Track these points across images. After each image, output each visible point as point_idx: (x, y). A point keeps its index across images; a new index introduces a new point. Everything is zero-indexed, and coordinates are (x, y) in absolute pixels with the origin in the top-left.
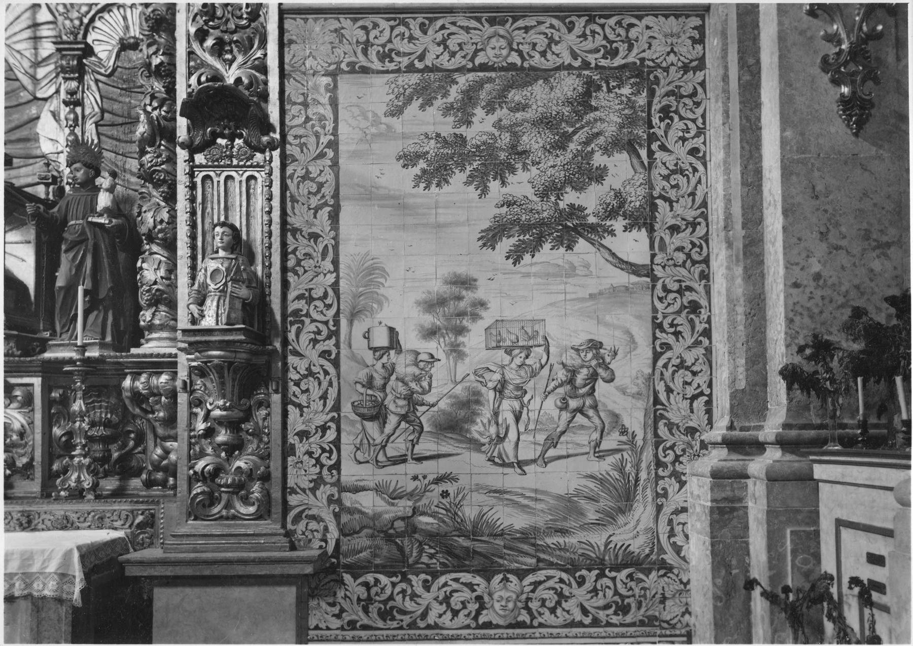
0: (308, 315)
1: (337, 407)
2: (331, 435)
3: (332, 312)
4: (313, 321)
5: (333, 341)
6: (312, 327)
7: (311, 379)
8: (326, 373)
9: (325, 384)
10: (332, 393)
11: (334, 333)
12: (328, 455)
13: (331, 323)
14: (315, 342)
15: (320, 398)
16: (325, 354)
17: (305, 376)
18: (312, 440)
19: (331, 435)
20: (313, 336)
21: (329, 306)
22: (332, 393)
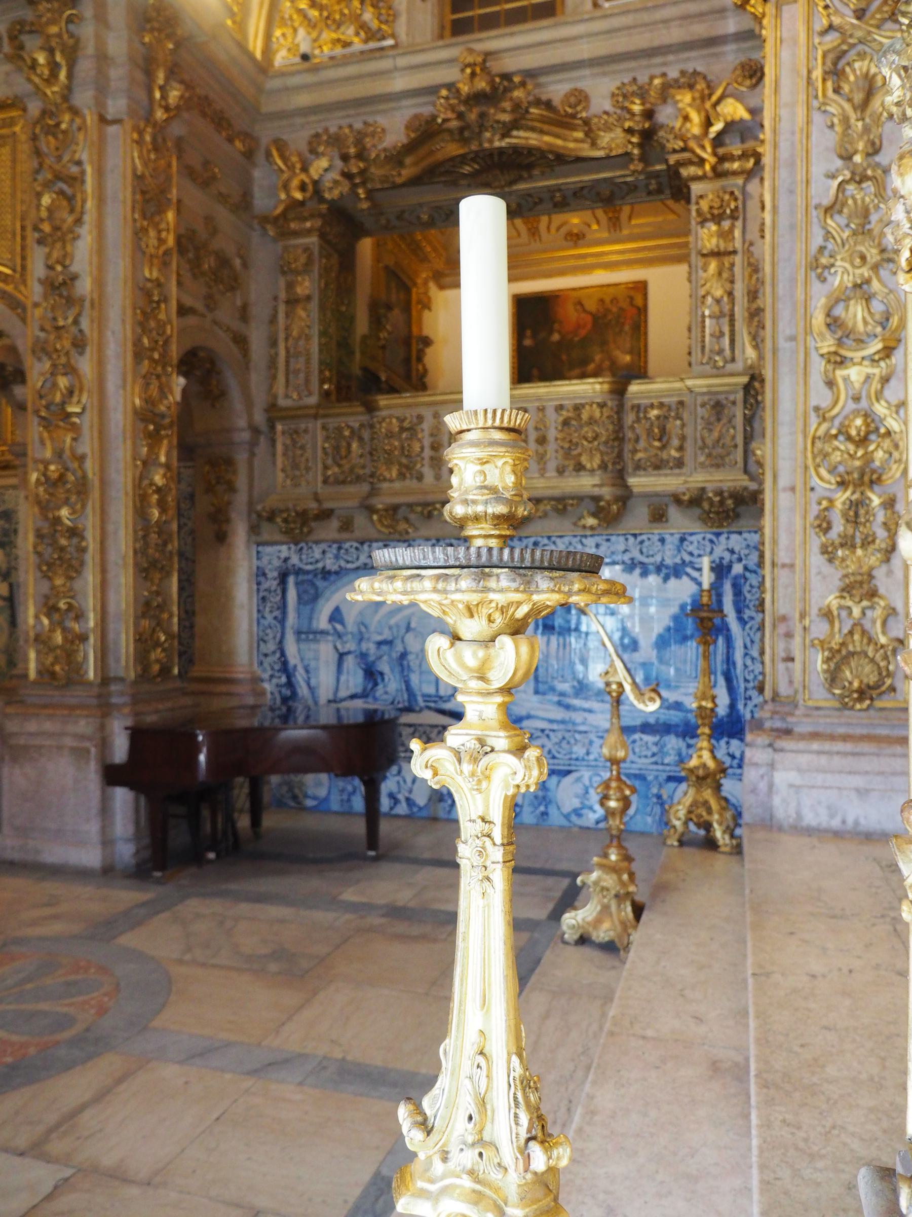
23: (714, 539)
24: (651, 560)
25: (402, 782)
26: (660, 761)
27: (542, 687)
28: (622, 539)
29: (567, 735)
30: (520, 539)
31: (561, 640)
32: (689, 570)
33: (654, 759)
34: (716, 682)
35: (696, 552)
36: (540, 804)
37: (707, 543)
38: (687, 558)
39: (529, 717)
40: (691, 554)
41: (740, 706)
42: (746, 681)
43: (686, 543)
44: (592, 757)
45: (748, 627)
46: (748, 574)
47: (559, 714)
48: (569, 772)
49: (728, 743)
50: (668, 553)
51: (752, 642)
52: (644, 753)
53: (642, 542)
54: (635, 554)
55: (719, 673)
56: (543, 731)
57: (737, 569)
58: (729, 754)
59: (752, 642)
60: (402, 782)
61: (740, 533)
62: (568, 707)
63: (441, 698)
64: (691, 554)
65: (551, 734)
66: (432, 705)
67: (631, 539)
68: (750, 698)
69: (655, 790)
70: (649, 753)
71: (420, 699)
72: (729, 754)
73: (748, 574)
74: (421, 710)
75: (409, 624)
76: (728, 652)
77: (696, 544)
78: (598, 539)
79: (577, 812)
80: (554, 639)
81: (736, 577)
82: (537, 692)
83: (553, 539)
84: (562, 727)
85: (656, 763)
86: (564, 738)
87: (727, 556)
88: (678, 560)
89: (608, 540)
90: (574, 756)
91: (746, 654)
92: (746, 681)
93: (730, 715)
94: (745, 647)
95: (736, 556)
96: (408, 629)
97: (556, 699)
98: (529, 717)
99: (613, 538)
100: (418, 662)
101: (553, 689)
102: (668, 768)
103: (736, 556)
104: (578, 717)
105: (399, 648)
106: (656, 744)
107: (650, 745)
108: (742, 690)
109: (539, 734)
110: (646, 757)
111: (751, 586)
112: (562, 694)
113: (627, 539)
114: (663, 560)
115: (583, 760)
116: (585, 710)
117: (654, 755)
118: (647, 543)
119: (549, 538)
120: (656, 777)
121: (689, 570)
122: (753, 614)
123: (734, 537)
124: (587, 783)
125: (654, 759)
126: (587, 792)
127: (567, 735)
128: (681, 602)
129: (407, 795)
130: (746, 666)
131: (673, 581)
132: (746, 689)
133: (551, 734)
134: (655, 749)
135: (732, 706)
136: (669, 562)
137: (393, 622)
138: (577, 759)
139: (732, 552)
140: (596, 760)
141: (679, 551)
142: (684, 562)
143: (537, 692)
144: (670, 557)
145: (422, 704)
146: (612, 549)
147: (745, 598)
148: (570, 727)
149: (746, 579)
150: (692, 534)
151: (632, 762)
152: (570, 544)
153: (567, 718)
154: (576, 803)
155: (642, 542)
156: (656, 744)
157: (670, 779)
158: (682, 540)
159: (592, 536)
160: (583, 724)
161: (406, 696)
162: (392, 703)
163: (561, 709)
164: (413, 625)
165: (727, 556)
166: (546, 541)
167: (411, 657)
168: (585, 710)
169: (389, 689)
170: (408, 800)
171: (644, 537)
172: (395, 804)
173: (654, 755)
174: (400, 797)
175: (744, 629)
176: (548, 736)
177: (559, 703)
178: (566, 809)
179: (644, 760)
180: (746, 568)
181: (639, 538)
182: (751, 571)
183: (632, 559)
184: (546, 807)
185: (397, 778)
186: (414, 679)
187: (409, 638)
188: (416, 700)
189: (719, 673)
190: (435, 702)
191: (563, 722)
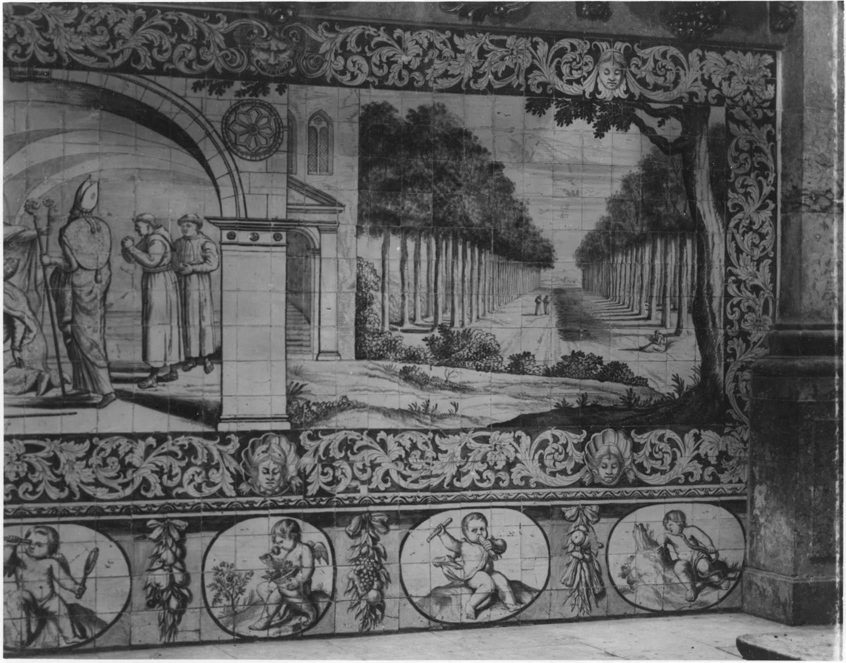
0: (180, 41)
1: (74, 66)
2: (42, 57)
3: (182, 67)
4: (174, 46)
5: (149, 67)
6: (167, 45)
7: (108, 39)
8: (115, 56)
9: (103, 54)
10: (89, 61)
11: (159, 69)
12: (19, 52)
13: (171, 67)
14: (150, 46)
15: (85, 47)
16: (135, 56)
17: (111, 31)
18: (37, 34)
19: (42, 57)
20: (156, 44)
21: (189, 65)
22: (89, 61)
23: (681, 56)
24: (575, 90)
25: (58, 573)
26: (587, 480)
27: (373, 343)
28: (524, 43)
29: (420, 439)
30: (331, 29)
31: (411, 245)
32: (640, 113)
33: (576, 477)
34: (679, 326)
35: (650, 79)
36: (368, 589)
37: (670, 65)
38: (636, 90)
39: (345, 405)
40: (642, 82)
41: (719, 370)
42: (728, 322)
43: (635, 60)
44: (466, 482)
45: (732, 224)
46: (733, 126)
47: (407, 397)
48: (428, 514)
49: (697, 437)
50: (604, 78)
51: (739, 251)
52: (559, 466)
53: (561, 52)
54: (548, 74)
55: (685, 309)
56: (373, 433)
57: (717, 115)
58: (698, 457)
59: (739, 251)
60: (58, 573)
61: (722, 52)
62: (422, 382)
63: (154, 371)
64: (642, 82)
65: (390, 440)
66: (133, 388)
67: (543, 48)
68: (734, 355)
69: (578, 537)
70: (570, 466)
71: (103, 374)
72: (698, 457)
73: (733, 126)
74: (106, 401)
75: (78, 199)
76: (700, 268)
77: (650, 64)
78: (485, 39)
79: (439, 596)
80: (395, 243)
81: (717, 129)
82: (360, 355)
83: (398, 32)
84: (412, 423)
85: (581, 484)
86: (414, 446)
87: (700, 89)
88: (620, 93)
89: (501, 44)
90: (435, 482)
91: (729, 274)
92: (728, 322)
93: (700, 387)
94: (728, 262)
95: (714, 92)
96: (76, 212)
97: (399, 366)
98: (345, 405)
99: (510, 40)
100: (98, 290)
101: (392, 346)
102: (601, 491)
103: (714, 92)
104: (442, 401)
105: (55, 256)
106: (580, 447)
107: (570, 449)
108: (720, 339)
109: (366, 440)
110: (563, 472)
111: (737, 149)
112: (412, 357)
113: (535, 45)
114: (596, 90)
115: (452, 488)
116: (454, 388)
117: (577, 468)
118: (569, 56)
119: (390, 30)
120: (581, 510)
121: (640, 113)
122: (741, 200)
123: (712, 56)
124: (459, 535)
125: (576, 477)
126: (459, 554)
127: (420, 439)
128: (626, 173)
129: (71, 599)
130: (727, 296)
131: (613, 135)
132: (727, 337)
133: (390, 440)
134: (578, 456)
135: (706, 368)
136: (606, 94)
137: (36, 194)
138: (439, 488)
139: (708, 84)
140: (473, 487)
141: (624, 76)
142: (632, 96)
143: (360, 355)
144: (607, 83)
145: (108, 388)
146: (508, 62)
147: (730, 171)
148: (427, 423)
149: (731, 136)
150: (643, 47)
151: (539, 485)
152: (431, 45)
153: (420, 403)
154: (439, 578)
155: (561, 52)
156: (580, 447)
157: (605, 511)
158: (629, 55)
159: (473, 32)
160: (451, 415)
161: (68, 371)
162: (35, 387)
163: (408, 388)
164: (88, 203)
165: (700, 89)
166: (383, 37)
167: (83, 279)
168: (454, 388)
169: (25, 355)
170: (73, 610)
171: (565, 43)
172: (42, 624)
173: (577, 468)
174: (53, 606)
175: (726, 227)
176: (383, 444)
177: (406, 376)
178: (419, 591)
179: (561, 480)
180: (729, 117)
181: (557, 46)
182: (739, 123)
183: (544, 85)
184: (380, 590)
185: (46, 564)
186: (89, 329)
187: (78, 234)
188: (95, 381)
189: (685, 309)
190: (140, 381)
191: (410, 413)
